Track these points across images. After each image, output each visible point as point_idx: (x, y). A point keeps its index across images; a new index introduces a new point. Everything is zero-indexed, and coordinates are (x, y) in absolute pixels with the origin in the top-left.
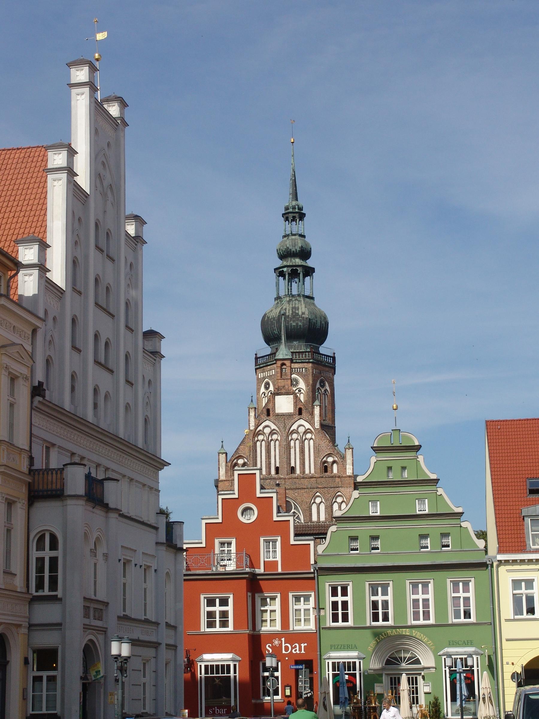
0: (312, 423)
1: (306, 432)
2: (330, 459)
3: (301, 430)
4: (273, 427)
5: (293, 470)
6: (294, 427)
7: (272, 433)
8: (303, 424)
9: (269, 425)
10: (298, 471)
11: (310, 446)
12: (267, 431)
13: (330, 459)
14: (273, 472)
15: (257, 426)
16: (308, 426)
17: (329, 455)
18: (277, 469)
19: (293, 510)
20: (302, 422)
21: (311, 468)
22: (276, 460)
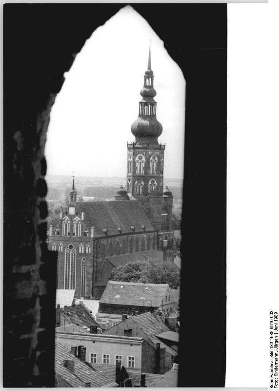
0: (81, 218)
1: (79, 221)
2: (86, 231)
3: (77, 220)
4: (68, 219)
5: (74, 234)
6: (75, 219)
7: (67, 220)
8: (77, 218)
9: (67, 218)
10: (76, 234)
11: (80, 226)
12: (66, 220)
13: (86, 231)
14: (67, 234)
15: (63, 218)
16: (79, 219)
17: (86, 230)
18: (69, 233)
19: (73, 248)
20: (77, 217)
21: (80, 234)
22: (68, 230)
